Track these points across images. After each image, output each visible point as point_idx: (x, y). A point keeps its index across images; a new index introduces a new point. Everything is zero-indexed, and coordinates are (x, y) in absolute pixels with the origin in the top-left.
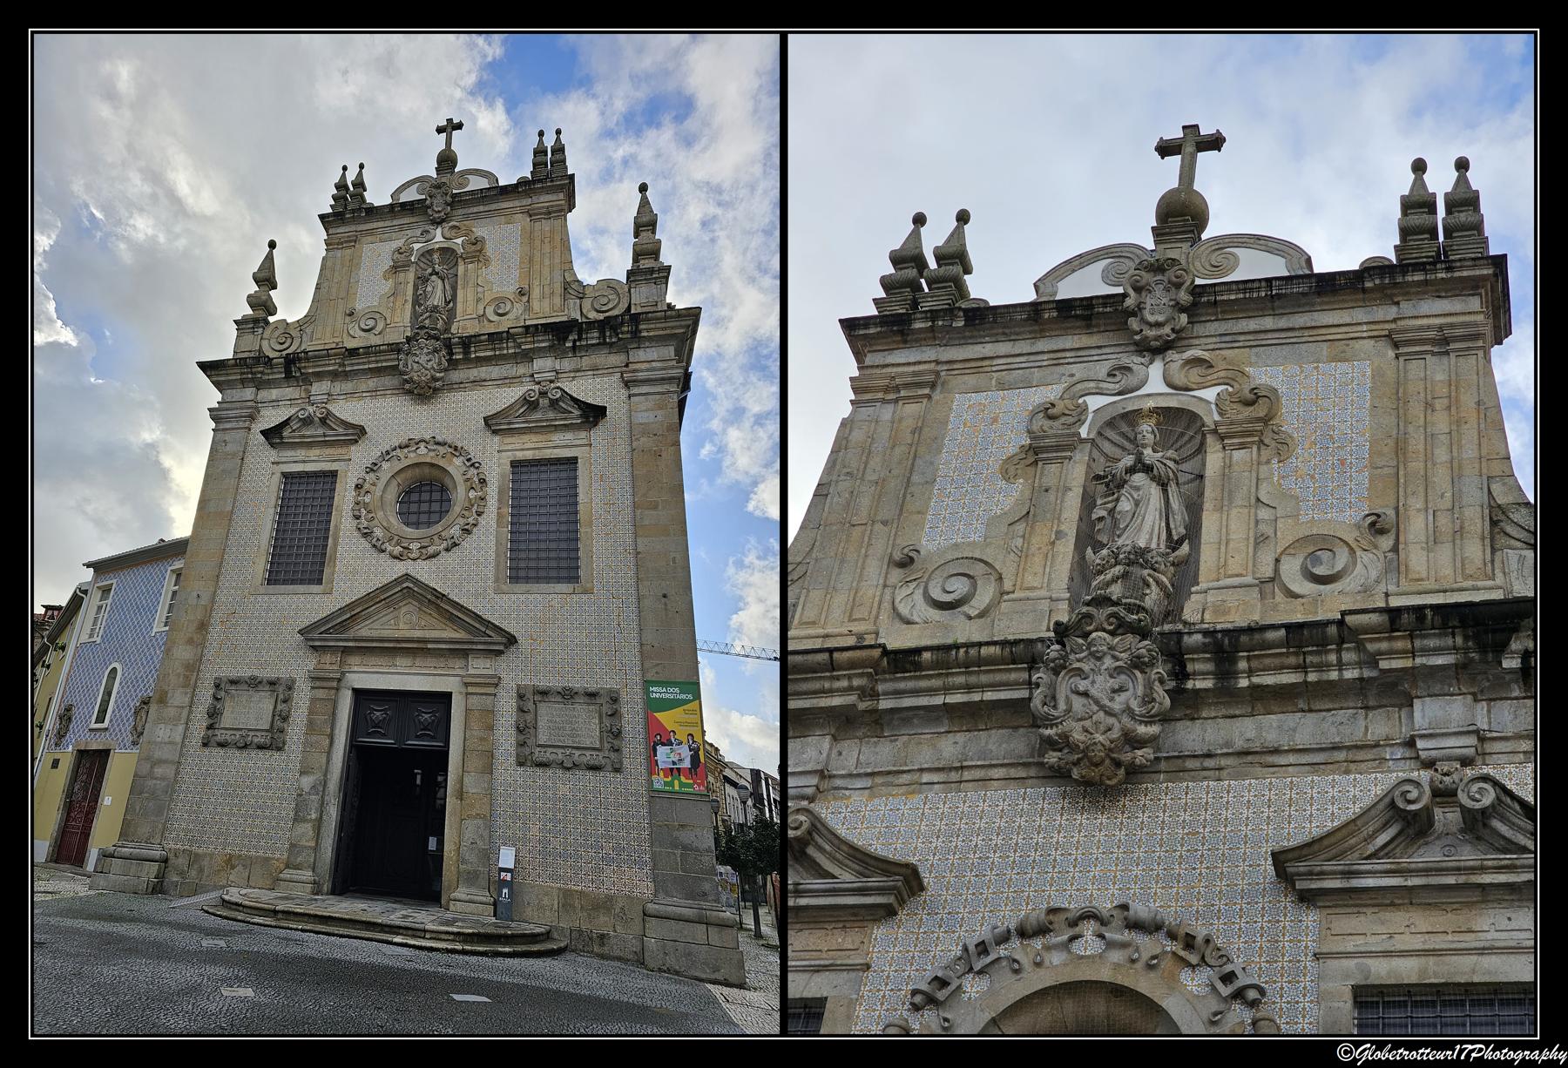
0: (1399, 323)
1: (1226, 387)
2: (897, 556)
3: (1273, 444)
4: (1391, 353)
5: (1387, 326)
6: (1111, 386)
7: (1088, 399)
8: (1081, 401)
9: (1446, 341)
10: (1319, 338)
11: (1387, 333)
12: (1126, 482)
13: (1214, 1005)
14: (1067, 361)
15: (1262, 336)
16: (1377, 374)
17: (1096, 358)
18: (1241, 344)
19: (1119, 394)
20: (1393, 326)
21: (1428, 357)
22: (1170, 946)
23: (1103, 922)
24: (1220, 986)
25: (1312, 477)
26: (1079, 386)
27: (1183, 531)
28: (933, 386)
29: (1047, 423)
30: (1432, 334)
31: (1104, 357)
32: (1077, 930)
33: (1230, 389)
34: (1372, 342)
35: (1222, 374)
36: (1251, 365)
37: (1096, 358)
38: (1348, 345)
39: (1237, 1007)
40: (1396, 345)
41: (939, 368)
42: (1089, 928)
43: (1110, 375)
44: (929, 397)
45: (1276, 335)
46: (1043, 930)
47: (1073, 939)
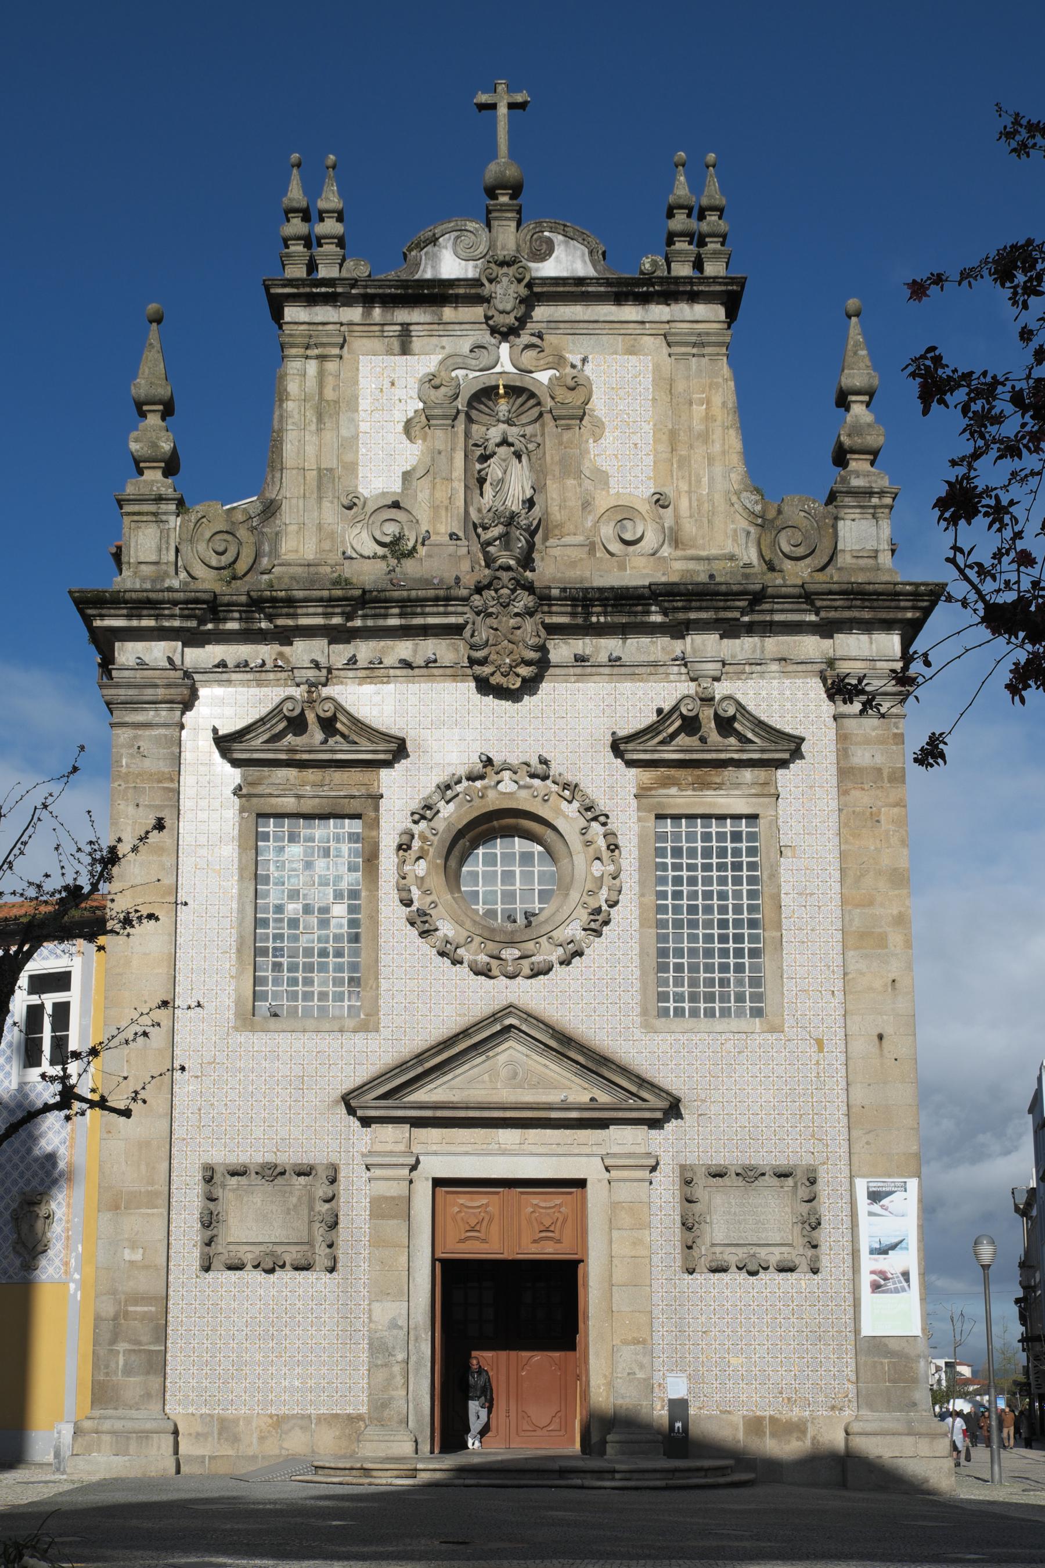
0: (673, 325)
1: (555, 371)
2: (346, 502)
3: (589, 426)
4: (665, 350)
5: (662, 326)
6: (474, 362)
7: (460, 373)
8: (453, 374)
9: (703, 345)
10: (615, 332)
11: (662, 332)
12: (495, 453)
13: (583, 823)
14: (437, 333)
15: (576, 325)
16: (657, 368)
17: (459, 333)
18: (561, 331)
19: (480, 370)
20: (667, 326)
21: (690, 357)
22: (555, 788)
23: (515, 773)
24: (583, 812)
25: (616, 456)
26: (450, 361)
27: (532, 491)
28: (342, 347)
29: (433, 391)
30: (693, 339)
31: (465, 333)
32: (498, 777)
33: (558, 374)
34: (651, 338)
35: (550, 359)
36: (570, 352)
37: (459, 333)
38: (635, 340)
39: (594, 824)
40: (669, 345)
41: (343, 328)
42: (506, 774)
43: (471, 351)
44: (341, 357)
45: (586, 325)
46: (482, 777)
47: (499, 782)
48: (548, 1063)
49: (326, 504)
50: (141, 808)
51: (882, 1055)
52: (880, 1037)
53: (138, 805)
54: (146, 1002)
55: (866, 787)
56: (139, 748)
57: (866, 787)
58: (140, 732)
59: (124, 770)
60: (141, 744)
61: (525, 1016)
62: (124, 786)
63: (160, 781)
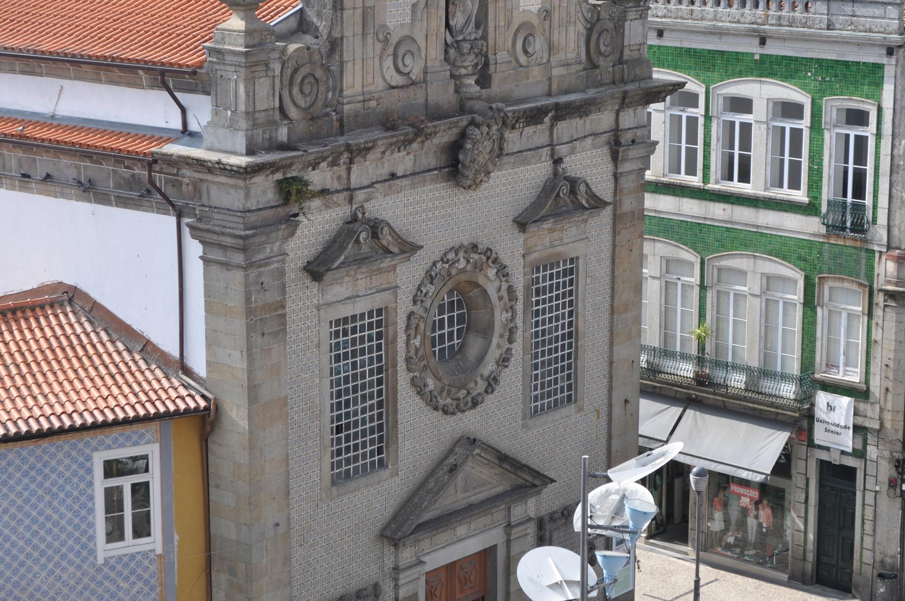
48: (483, 470)
49: (370, 40)
50: (265, 337)
51: (626, 414)
52: (626, 401)
53: (263, 334)
54: (274, 498)
55: (628, 226)
56: (262, 283)
57: (628, 226)
58: (262, 269)
59: (253, 305)
60: (263, 279)
61: (486, 447)
62: (254, 319)
63: (276, 310)
